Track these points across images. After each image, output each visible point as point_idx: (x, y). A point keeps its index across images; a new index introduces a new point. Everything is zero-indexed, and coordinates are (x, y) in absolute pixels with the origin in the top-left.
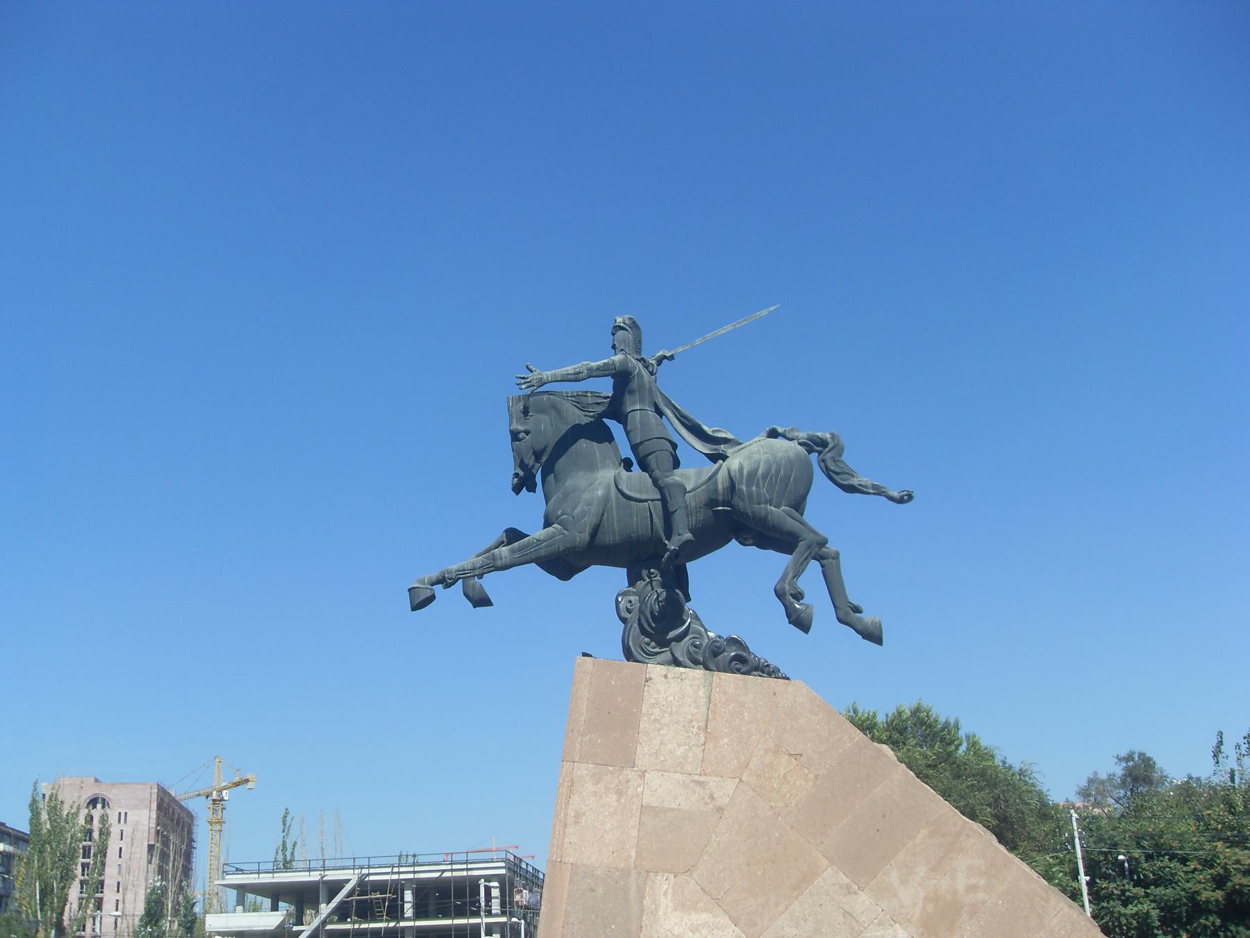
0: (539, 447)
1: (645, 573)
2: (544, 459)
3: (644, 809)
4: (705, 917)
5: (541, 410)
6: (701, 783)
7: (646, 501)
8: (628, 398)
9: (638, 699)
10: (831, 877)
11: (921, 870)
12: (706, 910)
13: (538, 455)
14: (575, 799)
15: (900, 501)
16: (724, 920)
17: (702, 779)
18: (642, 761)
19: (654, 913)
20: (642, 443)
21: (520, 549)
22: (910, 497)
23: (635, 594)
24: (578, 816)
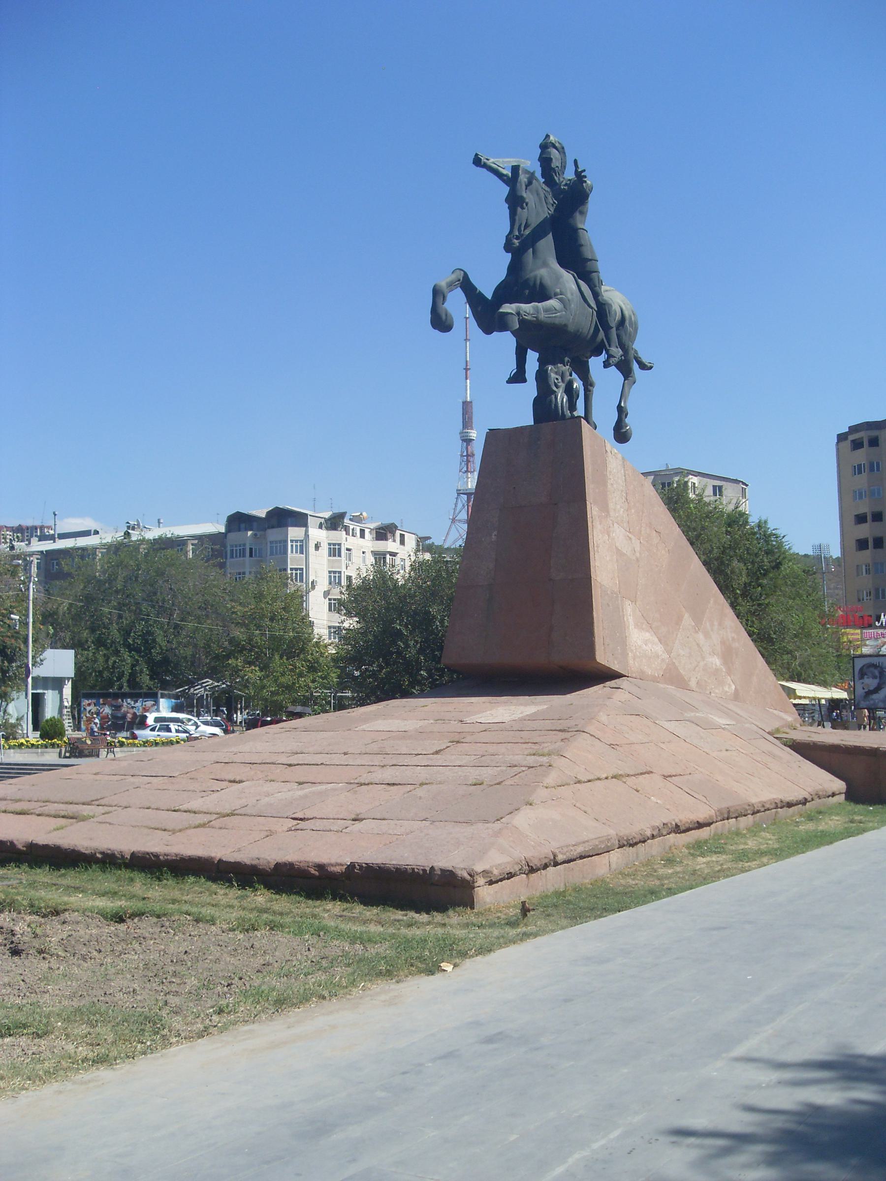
0: (529, 222)
1: (566, 359)
2: (527, 232)
3: (619, 552)
4: (647, 635)
5: (531, 191)
6: (630, 539)
7: (592, 308)
8: (577, 215)
9: (605, 464)
10: (687, 620)
11: (716, 623)
12: (648, 631)
13: (526, 226)
14: (595, 533)
15: (643, 366)
16: (656, 640)
17: (630, 535)
18: (612, 513)
19: (628, 627)
20: (591, 260)
21: (546, 310)
22: (651, 368)
23: (556, 373)
24: (598, 547)
